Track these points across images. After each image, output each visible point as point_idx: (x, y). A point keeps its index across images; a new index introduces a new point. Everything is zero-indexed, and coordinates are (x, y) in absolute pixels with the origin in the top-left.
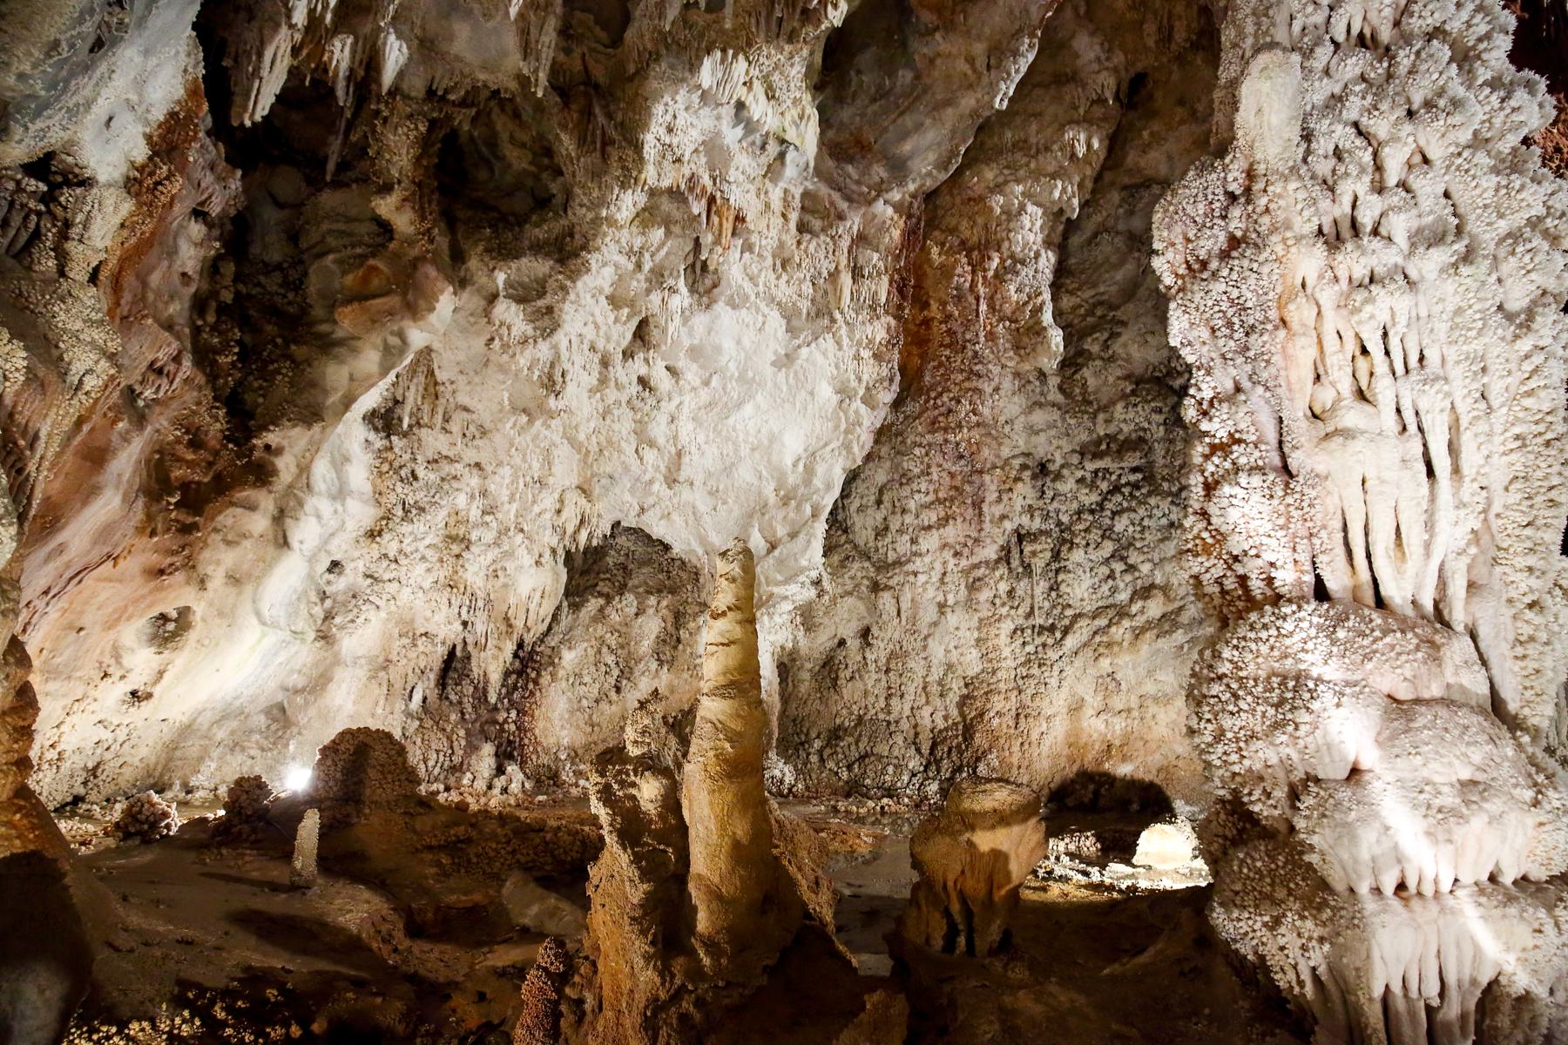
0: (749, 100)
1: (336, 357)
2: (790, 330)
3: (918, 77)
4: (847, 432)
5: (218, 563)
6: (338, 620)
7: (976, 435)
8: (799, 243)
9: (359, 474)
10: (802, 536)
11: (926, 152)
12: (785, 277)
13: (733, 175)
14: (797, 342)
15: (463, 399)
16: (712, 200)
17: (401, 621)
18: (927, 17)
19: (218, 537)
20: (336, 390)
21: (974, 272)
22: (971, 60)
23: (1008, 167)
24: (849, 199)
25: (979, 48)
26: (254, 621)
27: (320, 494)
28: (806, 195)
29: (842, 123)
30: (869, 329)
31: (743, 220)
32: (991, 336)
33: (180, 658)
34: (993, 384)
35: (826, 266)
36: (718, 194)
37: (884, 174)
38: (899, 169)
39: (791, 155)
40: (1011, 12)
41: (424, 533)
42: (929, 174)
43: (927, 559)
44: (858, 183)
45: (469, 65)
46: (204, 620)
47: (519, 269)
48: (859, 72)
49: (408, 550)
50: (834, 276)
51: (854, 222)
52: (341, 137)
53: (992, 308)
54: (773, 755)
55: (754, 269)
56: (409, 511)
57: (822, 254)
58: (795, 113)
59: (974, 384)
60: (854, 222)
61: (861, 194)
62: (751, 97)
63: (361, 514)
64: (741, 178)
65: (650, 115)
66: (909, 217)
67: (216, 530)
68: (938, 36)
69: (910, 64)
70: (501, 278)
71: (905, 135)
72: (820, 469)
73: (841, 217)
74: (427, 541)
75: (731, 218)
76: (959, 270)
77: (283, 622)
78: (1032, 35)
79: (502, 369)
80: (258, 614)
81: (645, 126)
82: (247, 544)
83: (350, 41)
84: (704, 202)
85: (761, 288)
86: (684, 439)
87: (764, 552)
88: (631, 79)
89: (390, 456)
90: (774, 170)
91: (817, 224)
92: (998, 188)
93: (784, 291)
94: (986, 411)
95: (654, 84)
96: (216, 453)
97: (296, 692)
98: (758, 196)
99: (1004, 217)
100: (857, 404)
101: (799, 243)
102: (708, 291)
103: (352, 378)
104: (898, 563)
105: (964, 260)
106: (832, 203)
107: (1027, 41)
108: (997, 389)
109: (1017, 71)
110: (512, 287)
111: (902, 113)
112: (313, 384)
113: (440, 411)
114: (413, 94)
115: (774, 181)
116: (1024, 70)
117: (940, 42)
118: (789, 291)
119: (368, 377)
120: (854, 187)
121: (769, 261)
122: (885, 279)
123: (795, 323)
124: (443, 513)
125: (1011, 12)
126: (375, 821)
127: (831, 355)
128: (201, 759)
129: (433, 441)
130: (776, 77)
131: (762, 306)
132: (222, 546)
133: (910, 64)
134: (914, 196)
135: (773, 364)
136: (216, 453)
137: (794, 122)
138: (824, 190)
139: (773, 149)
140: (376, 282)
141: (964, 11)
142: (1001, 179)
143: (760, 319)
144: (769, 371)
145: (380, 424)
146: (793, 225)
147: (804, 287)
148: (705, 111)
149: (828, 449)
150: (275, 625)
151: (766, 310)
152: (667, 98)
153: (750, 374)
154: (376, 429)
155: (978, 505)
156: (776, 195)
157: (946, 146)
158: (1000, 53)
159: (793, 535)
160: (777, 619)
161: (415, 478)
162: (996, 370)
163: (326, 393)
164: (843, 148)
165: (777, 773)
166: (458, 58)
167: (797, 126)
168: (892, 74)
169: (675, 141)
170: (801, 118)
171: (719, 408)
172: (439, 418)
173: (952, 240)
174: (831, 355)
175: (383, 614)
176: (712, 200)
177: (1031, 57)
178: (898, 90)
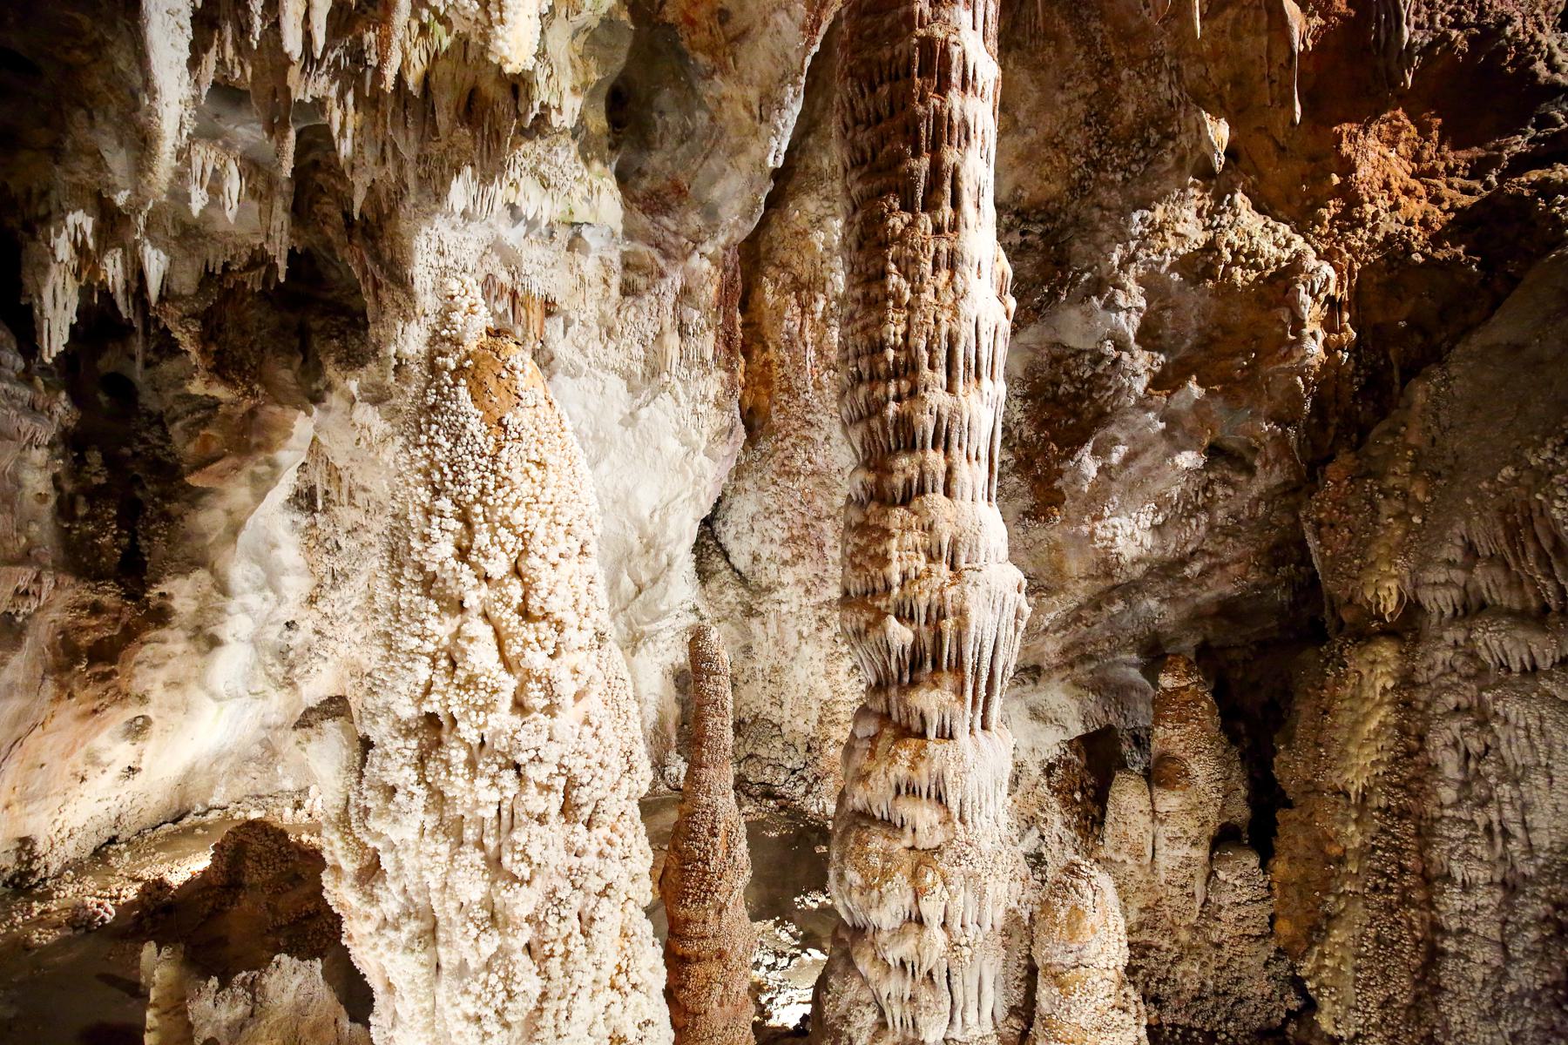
0: (519, 200)
1: (204, 506)
2: (631, 390)
3: (712, 119)
4: (696, 483)
5: (153, 681)
6: (298, 671)
7: (810, 484)
8: (619, 311)
9: (290, 553)
10: (661, 582)
11: (734, 198)
12: (612, 345)
13: (527, 268)
14: (638, 401)
15: (359, 480)
16: (514, 294)
17: (348, 665)
18: (703, 59)
19: (144, 667)
20: (215, 529)
21: (803, 313)
22: (747, 106)
23: (827, 198)
24: (666, 255)
25: (753, 94)
26: (209, 701)
27: (244, 592)
28: (624, 255)
29: (655, 170)
30: (702, 385)
31: (554, 303)
32: (818, 386)
33: (150, 746)
34: (824, 434)
35: (650, 329)
36: (519, 288)
37: (701, 223)
38: (711, 213)
39: (586, 233)
40: (773, 55)
41: (350, 596)
42: (736, 225)
43: (788, 590)
44: (676, 234)
45: (241, 236)
46: (159, 717)
47: (369, 373)
48: (661, 113)
49: (339, 613)
50: (659, 336)
51: (675, 279)
52: (141, 337)
53: (821, 353)
54: (673, 754)
55: (581, 341)
56: (338, 578)
57: (644, 318)
58: (582, 189)
59: (806, 433)
60: (675, 279)
61: (680, 247)
62: (520, 196)
63: (296, 586)
64: (538, 268)
65: (411, 253)
66: (726, 270)
67: (140, 663)
68: (717, 78)
69: (702, 105)
70: (353, 386)
71: (713, 181)
72: (672, 521)
73: (662, 275)
74: (354, 604)
75: (537, 309)
76: (788, 314)
77: (241, 690)
78: (795, 83)
79: (374, 462)
80: (215, 697)
81: (410, 263)
82: (174, 660)
83: (118, 256)
84: (506, 296)
85: (591, 358)
87: (632, 596)
88: (389, 217)
89: (314, 532)
90: (575, 244)
91: (641, 282)
92: (819, 222)
93: (615, 357)
94: (819, 460)
95: (403, 225)
96: (120, 611)
97: (277, 728)
98: (571, 271)
99: (827, 254)
100: (700, 457)
101: (619, 311)
102: (547, 364)
103: (229, 513)
104: (769, 590)
105: (794, 301)
106: (653, 259)
107: (790, 89)
108: (827, 439)
109: (785, 125)
110: (366, 390)
111: (706, 158)
112: (186, 537)
113: (345, 492)
114: (184, 292)
115: (585, 250)
116: (792, 123)
117: (721, 86)
118: (621, 356)
119: (246, 506)
120: (672, 240)
121: (596, 330)
122: (711, 335)
123: (634, 382)
124: (364, 578)
125: (773, 55)
126: (246, 904)
127: (671, 412)
128: (211, 787)
129: (348, 516)
130: (543, 168)
131: (598, 372)
132: (151, 671)
133: (702, 105)
134: (726, 248)
135: (621, 423)
136: (120, 611)
137: (585, 199)
138: (642, 248)
139: (563, 235)
140: (214, 446)
141: (734, 55)
142: (821, 212)
143: (600, 384)
144: (618, 429)
145: (304, 503)
146: (615, 292)
147: (634, 351)
148: (472, 226)
149: (680, 500)
150: (233, 695)
151: (603, 376)
152: (425, 229)
153: (602, 434)
154: (301, 508)
155: (820, 547)
156: (590, 266)
157: (747, 195)
158: (769, 103)
159: (655, 581)
160: (660, 645)
161: (339, 548)
162: (826, 419)
163: (204, 536)
164: (650, 199)
165: (674, 770)
166: (227, 234)
167: (588, 201)
168: (690, 115)
169: (450, 262)
170: (590, 192)
172: (345, 498)
173: (785, 278)
174: (671, 412)
175: (330, 663)
176: (514, 294)
177: (797, 108)
178: (699, 132)
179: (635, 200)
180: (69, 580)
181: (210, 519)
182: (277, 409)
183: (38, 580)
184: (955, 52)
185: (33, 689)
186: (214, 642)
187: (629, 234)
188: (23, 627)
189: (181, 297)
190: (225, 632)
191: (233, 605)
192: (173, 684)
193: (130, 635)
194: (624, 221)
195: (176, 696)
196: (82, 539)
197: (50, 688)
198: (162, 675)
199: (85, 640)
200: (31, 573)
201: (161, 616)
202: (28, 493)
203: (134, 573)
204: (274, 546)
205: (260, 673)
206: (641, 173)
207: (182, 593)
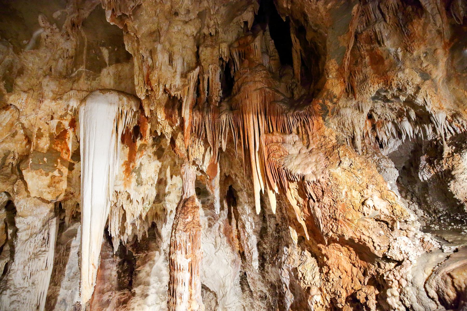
77: (154, 303)
80: (149, 306)
86: (205, 269)
91: (212, 223)
146: (207, 226)
171: (209, 262)
179: (208, 207)
180: (117, 292)
181: (142, 275)
182: (152, 252)
184: (175, 262)
186: (147, 295)
187: (206, 215)
188: (110, 302)
189: (130, 242)
190: (149, 293)
191: (150, 287)
192: (139, 305)
193: (129, 298)
194: (205, 213)
195: (140, 307)
196: (122, 281)
198: (136, 304)
199: (122, 300)
200: (111, 292)
201: (134, 294)
202: (113, 276)
203: (130, 286)
204: (161, 271)
205: (159, 299)
206: (208, 200)
207: (137, 290)
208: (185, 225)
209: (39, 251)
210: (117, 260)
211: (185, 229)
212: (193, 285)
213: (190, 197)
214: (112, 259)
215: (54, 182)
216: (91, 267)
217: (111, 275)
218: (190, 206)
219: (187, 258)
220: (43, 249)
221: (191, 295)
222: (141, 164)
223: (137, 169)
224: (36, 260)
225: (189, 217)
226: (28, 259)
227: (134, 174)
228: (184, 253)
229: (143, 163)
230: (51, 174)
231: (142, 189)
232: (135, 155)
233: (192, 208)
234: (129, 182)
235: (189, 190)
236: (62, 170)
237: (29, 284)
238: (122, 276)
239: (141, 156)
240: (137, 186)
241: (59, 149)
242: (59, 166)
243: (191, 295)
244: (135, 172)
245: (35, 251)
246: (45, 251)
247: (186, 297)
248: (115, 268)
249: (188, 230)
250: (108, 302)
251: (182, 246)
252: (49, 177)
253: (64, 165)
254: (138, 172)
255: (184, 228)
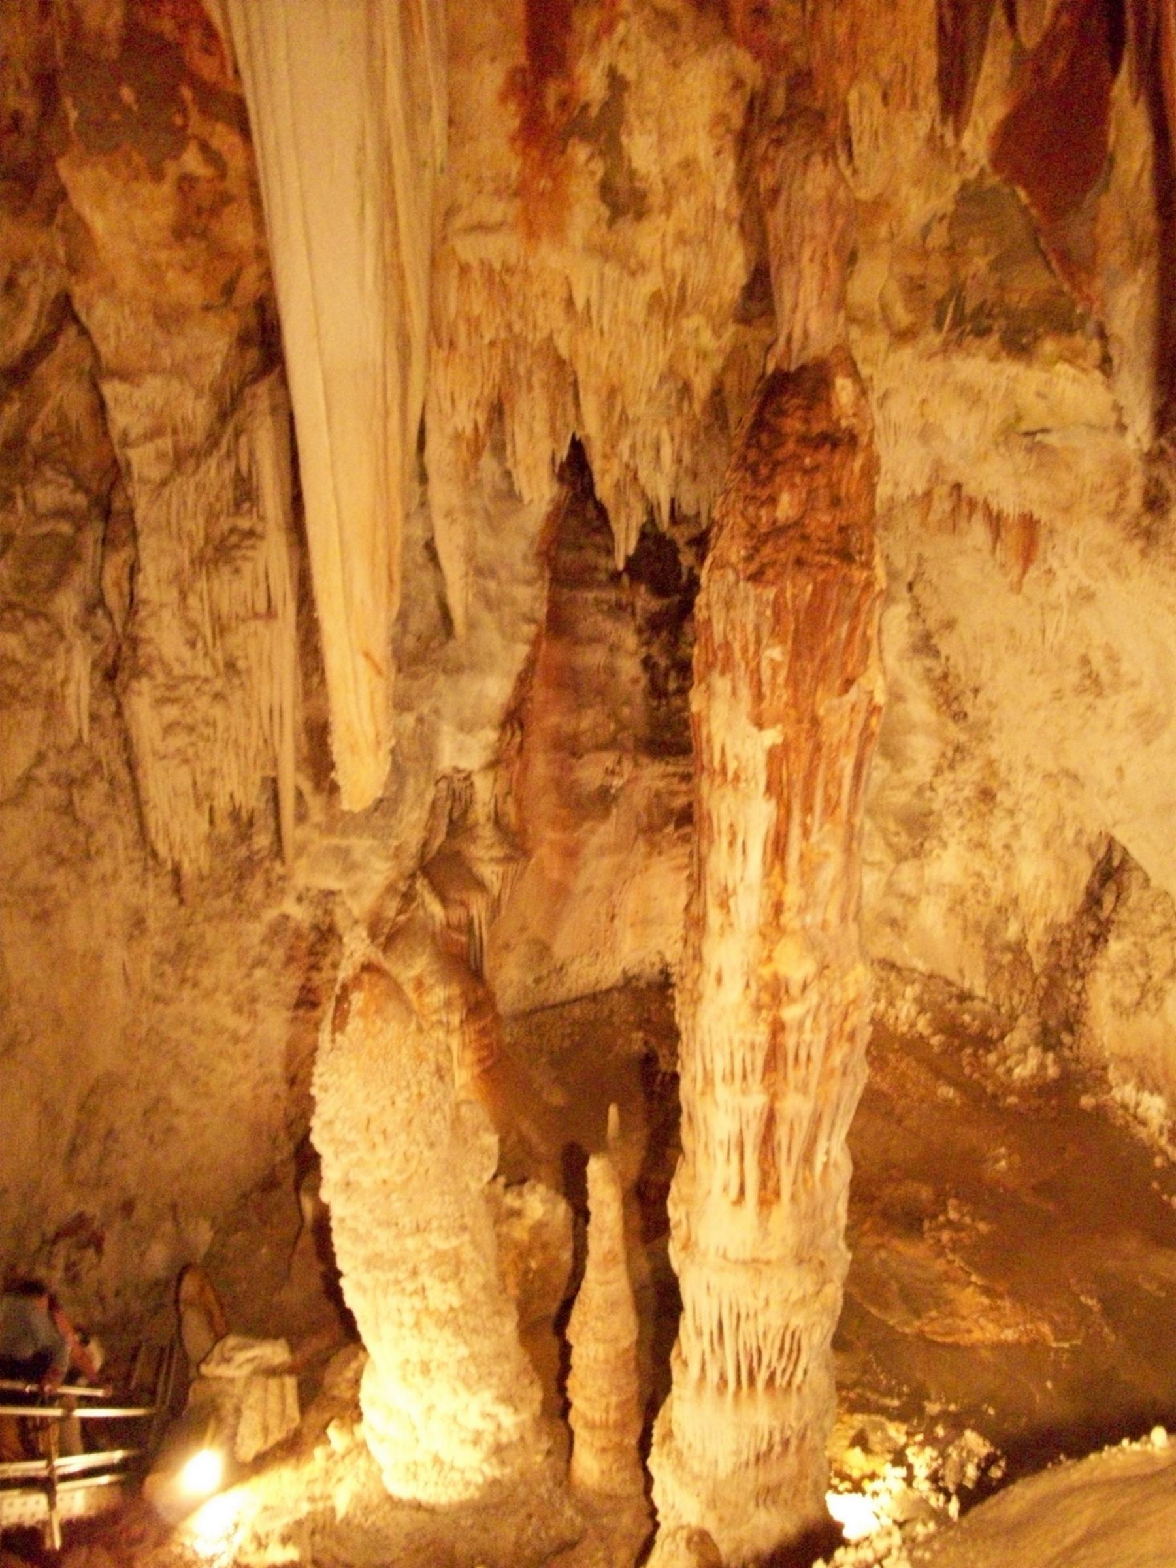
124: (977, 764)
146: (1134, 501)
180: (644, 760)
183: (619, 762)
185: (617, 848)
188: (615, 798)
197: (642, 847)
202: (624, 678)
208: (758, 539)
209: (232, 531)
210: (639, 604)
211: (753, 567)
212: (793, 858)
213: (802, 368)
214: (611, 595)
215: (199, 211)
216: (361, 662)
217: (612, 672)
218: (793, 425)
219: (760, 724)
220: (244, 524)
221: (778, 908)
222: (616, 83)
223: (594, 111)
224: (226, 571)
225: (785, 498)
226: (192, 562)
227: (580, 153)
228: (745, 692)
229: (630, 74)
230: (172, 170)
231: (648, 238)
232: (567, 26)
233: (803, 440)
234: (558, 200)
235: (799, 315)
236: (215, 143)
237: (214, 664)
238: (672, 686)
239: (608, 28)
240: (612, 222)
241: (167, 26)
242: (196, 123)
243: (778, 908)
244: (585, 136)
245: (216, 533)
246: (251, 533)
247: (749, 907)
248: (631, 641)
249: (770, 574)
250: (604, 799)
251: (738, 654)
252: (167, 188)
253: (217, 118)
254: (605, 130)
255: (749, 559)
